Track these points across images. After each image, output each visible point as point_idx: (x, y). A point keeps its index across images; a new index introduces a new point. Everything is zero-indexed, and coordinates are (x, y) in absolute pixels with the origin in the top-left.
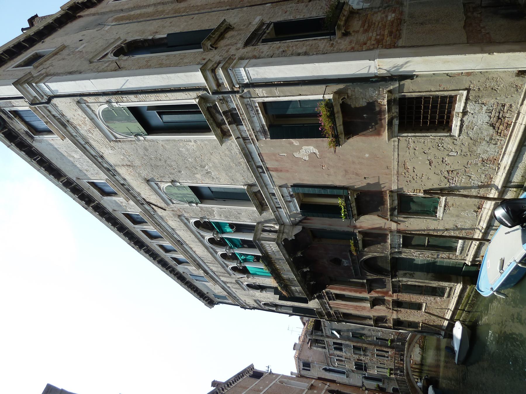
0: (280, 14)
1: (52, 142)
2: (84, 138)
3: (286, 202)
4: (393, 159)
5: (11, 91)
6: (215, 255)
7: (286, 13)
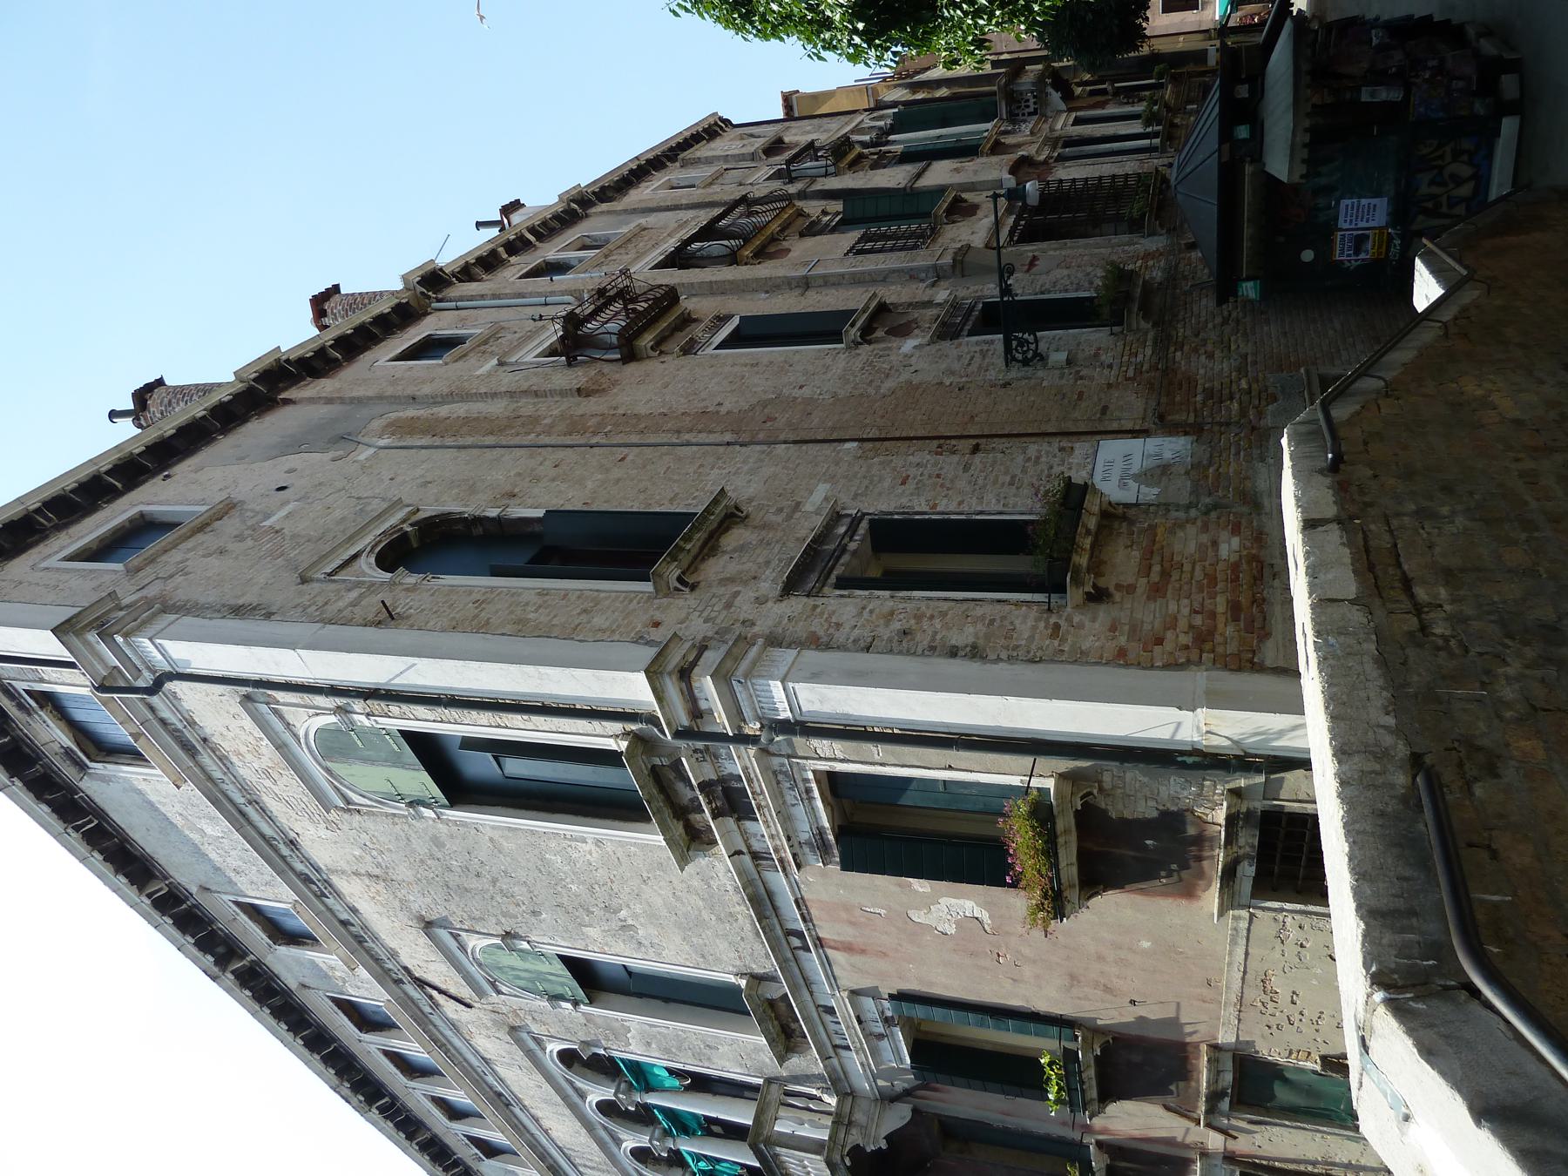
0: (886, 484)
1: (142, 786)
2: (244, 788)
3: (869, 1035)
4: (1230, 964)
5: (45, 644)
6: (614, 1149)
7: (903, 483)
